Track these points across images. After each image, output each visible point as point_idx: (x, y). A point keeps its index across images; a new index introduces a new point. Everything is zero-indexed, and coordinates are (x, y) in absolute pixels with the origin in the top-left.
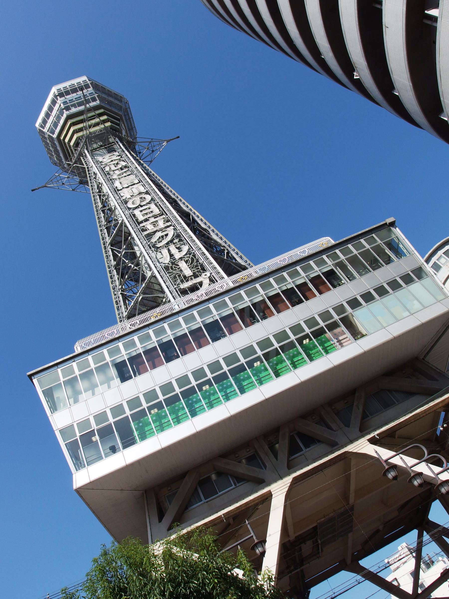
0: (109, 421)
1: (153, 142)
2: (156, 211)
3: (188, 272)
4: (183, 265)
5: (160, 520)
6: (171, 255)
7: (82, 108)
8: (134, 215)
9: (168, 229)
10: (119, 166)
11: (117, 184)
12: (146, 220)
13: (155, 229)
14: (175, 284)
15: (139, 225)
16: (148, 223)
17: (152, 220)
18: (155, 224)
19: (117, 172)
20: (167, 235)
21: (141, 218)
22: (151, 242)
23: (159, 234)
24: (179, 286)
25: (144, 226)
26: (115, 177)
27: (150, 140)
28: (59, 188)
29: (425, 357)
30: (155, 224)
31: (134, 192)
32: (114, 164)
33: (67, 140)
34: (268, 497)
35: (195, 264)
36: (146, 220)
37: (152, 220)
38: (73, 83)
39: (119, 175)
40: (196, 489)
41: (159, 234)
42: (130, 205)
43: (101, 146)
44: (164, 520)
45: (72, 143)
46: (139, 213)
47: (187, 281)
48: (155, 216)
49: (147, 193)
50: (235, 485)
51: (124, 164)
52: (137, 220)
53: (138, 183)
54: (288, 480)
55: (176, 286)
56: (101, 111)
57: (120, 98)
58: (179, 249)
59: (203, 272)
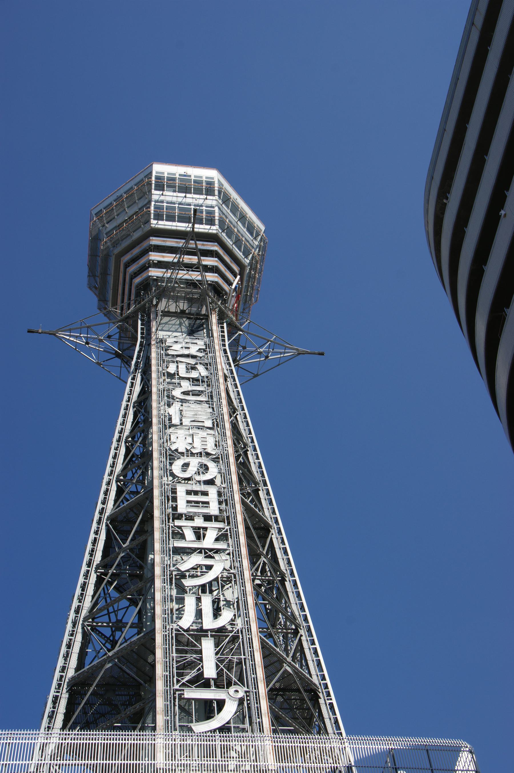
2: (214, 509)
6: (199, 613)
7: (182, 226)
8: (174, 491)
9: (217, 556)
10: (194, 374)
12: (190, 518)
14: (178, 681)
15: (173, 520)
16: (190, 523)
17: (199, 522)
19: (186, 386)
20: (209, 567)
21: (182, 508)
22: (177, 568)
23: (196, 559)
24: (183, 690)
25: (180, 527)
26: (177, 393)
28: (76, 349)
31: (195, 445)
35: (230, 656)
36: (190, 518)
38: (189, 173)
41: (196, 559)
42: (177, 467)
43: (183, 312)
45: (137, 280)
48: (208, 518)
49: (216, 460)
52: (175, 509)
56: (215, 247)
58: (217, 613)
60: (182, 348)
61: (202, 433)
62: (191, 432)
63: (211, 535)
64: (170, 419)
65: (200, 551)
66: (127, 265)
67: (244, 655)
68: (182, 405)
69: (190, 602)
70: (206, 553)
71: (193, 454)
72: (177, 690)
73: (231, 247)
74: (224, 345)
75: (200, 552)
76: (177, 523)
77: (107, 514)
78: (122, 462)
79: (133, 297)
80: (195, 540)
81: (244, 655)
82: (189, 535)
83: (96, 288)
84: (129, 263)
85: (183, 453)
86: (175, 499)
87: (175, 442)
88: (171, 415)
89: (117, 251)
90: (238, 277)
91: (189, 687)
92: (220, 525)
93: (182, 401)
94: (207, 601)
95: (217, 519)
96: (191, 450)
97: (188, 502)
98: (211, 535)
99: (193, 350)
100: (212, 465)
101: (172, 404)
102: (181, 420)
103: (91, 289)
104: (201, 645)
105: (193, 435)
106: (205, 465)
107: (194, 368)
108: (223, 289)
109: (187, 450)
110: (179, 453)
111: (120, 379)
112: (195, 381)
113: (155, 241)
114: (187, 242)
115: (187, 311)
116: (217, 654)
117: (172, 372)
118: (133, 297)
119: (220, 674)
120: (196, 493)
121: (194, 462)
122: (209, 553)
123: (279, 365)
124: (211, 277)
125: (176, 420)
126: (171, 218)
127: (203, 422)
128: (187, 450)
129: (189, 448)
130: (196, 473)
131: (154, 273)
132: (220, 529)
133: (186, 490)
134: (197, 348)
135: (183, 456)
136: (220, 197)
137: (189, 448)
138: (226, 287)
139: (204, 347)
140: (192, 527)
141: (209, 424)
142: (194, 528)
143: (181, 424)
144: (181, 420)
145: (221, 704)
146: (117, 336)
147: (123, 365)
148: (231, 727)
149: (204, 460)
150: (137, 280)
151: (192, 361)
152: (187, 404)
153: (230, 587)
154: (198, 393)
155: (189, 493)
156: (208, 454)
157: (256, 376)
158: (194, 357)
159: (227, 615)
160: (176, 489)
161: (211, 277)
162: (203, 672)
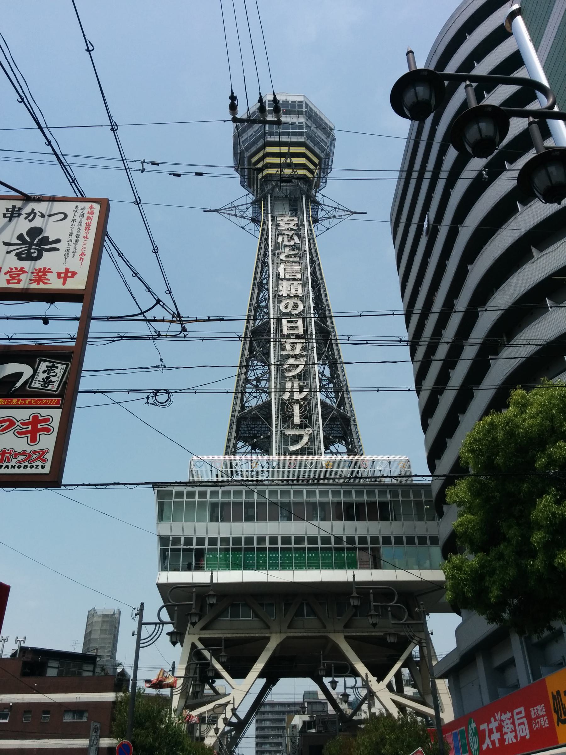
1: (338, 209)
2: (300, 331)
3: (297, 420)
4: (296, 409)
9: (302, 359)
10: (292, 243)
13: (291, 353)
14: (283, 426)
18: (293, 344)
19: (287, 250)
20: (298, 365)
21: (285, 331)
23: (292, 361)
27: (335, 205)
30: (293, 344)
31: (292, 291)
32: (288, 235)
34: (268, 639)
39: (287, 256)
40: (227, 609)
41: (292, 361)
46: (286, 322)
47: (293, 428)
48: (298, 336)
49: (302, 299)
50: (253, 618)
53: (300, 280)
54: (284, 636)
57: (327, 130)
58: (301, 391)
61: (296, 283)
62: (290, 283)
63: (298, 347)
65: (292, 356)
72: (283, 430)
73: (313, 148)
75: (293, 357)
77: (250, 329)
79: (259, 187)
82: (288, 346)
94: (296, 384)
98: (298, 347)
99: (291, 226)
100: (300, 303)
108: (309, 178)
109: (288, 295)
110: (284, 297)
112: (293, 248)
113: (269, 149)
114: (286, 160)
118: (259, 187)
121: (291, 302)
122: (297, 357)
125: (282, 276)
128: (288, 295)
132: (303, 343)
134: (294, 223)
136: (306, 116)
137: (289, 293)
138: (310, 175)
141: (299, 276)
145: (301, 437)
147: (256, 229)
149: (296, 300)
157: (328, 229)
161: (301, 172)
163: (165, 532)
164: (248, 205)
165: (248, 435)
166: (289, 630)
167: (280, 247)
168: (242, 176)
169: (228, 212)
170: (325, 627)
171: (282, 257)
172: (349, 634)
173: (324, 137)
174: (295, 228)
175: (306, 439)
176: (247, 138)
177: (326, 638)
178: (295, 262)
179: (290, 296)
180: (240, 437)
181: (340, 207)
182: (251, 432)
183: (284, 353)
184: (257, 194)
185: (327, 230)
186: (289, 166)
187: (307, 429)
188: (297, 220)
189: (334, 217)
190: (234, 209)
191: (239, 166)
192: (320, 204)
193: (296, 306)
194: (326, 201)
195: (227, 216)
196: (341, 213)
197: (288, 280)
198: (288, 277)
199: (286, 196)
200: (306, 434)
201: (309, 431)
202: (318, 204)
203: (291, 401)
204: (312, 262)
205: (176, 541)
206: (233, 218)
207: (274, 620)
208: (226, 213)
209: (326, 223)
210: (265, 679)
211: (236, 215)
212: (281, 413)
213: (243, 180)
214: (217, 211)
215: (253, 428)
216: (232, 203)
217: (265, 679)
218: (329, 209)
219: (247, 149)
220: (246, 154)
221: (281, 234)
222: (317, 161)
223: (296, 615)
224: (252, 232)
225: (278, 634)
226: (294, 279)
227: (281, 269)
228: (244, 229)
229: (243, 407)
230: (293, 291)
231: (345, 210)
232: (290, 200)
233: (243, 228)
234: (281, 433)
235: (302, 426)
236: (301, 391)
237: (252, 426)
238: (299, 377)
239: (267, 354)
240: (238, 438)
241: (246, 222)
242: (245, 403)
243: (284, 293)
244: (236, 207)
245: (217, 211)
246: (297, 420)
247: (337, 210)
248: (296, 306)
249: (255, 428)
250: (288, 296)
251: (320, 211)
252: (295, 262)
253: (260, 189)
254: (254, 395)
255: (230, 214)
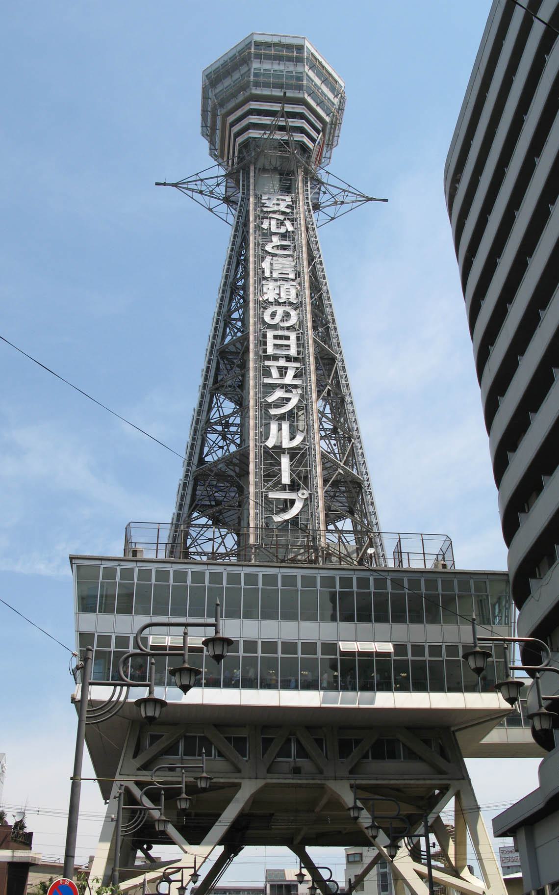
0: (129, 649)
2: (293, 352)
3: (286, 479)
4: (285, 461)
5: (135, 756)
6: (280, 437)
7: (278, 93)
8: (265, 336)
9: (294, 391)
10: (282, 230)
11: (266, 265)
14: (265, 486)
18: (282, 371)
19: (276, 240)
20: (289, 399)
21: (270, 350)
22: (265, 400)
23: (279, 394)
25: (268, 367)
27: (345, 187)
29: (457, 730)
30: (282, 371)
33: (236, 129)
34: (237, 787)
37: (282, 363)
41: (279, 394)
44: (139, 757)
45: (240, 140)
48: (289, 359)
49: (297, 306)
50: (215, 757)
51: (290, 228)
52: (265, 351)
53: (293, 280)
54: (260, 783)
55: (263, 490)
58: (292, 438)
59: (303, 488)
60: (274, 204)
61: (287, 285)
62: (278, 283)
63: (291, 373)
64: (263, 272)
65: (282, 386)
66: (232, 125)
67: (310, 467)
68: (272, 259)
69: (274, 427)
70: (286, 388)
71: (279, 304)
74: (307, 199)
75: (282, 388)
76: (267, 363)
77: (217, 348)
78: (227, 303)
79: (236, 154)
80: (279, 377)
81: (310, 467)
82: (275, 373)
83: (207, 135)
84: (233, 123)
85: (272, 302)
86: (265, 343)
87: (266, 293)
88: (264, 269)
89: (224, 111)
90: (321, 133)
91: (271, 490)
92: (297, 365)
93: (274, 255)
94: (285, 426)
95: (296, 360)
96: (279, 300)
97: (275, 345)
98: (291, 373)
99: (282, 208)
100: (293, 313)
101: (265, 257)
102: (271, 273)
103: (204, 137)
104: (280, 459)
105: (280, 287)
106: (289, 313)
107: (282, 224)
108: (308, 147)
111: (226, 222)
112: (284, 236)
113: (254, 105)
115: (279, 168)
116: (291, 466)
117: (266, 228)
118: (236, 154)
119: (293, 481)
120: (281, 337)
121: (280, 310)
122: (287, 388)
123: (352, 209)
124: (298, 137)
125: (267, 274)
126: (267, 85)
127: (288, 274)
129: (276, 299)
130: (281, 320)
131: (254, 134)
132: (297, 368)
133: (274, 335)
135: (272, 305)
138: (310, 145)
139: (291, 203)
140: (277, 366)
141: (292, 276)
142: (278, 367)
143: (271, 276)
144: (271, 273)
145: (293, 502)
146: (224, 184)
147: (229, 212)
148: (257, 657)
149: (288, 309)
150: (240, 140)
151: (281, 217)
152: (277, 258)
153: (303, 414)
154: (284, 248)
155: (275, 337)
156: (291, 304)
157: (333, 219)
158: (283, 213)
159: (299, 438)
160: (266, 334)
161: (298, 137)
162: (281, 479)
163: (87, 628)
164: (219, 178)
165: (208, 503)
166: (269, 775)
167: (267, 235)
168: (212, 142)
169: (190, 187)
170: (321, 772)
171: (268, 248)
172: (358, 782)
173: (331, 96)
174: (288, 211)
175: (298, 506)
176: (223, 89)
177: (322, 787)
178: (289, 256)
179: (279, 302)
180: (197, 505)
181: (351, 190)
182: (212, 498)
183: (267, 381)
184: (233, 165)
185: (331, 220)
186: (282, 128)
187: (301, 491)
188: (290, 200)
189: (342, 203)
190: (199, 183)
191: (210, 130)
192: (323, 183)
193: (287, 315)
194: (332, 180)
195: (189, 193)
196: (352, 198)
197: (276, 280)
198: (275, 275)
199: (275, 169)
200: (299, 498)
201: (304, 494)
202: (321, 183)
203: (279, 449)
204: (311, 258)
205: (105, 640)
206: (197, 196)
207: (247, 761)
208: (188, 189)
209: (330, 211)
210: (223, 846)
211: (201, 192)
212: (263, 467)
213: (212, 147)
214: (175, 185)
215: (216, 492)
216: (197, 174)
217: (223, 846)
218: (335, 191)
219: (221, 105)
220: (220, 111)
221: (267, 218)
222: (319, 126)
223: (279, 755)
224: (224, 216)
225: (254, 781)
226: (286, 280)
227: (266, 265)
228: (212, 211)
229: (201, 461)
230: (282, 295)
231: (357, 194)
232: (281, 174)
233: (210, 210)
234: (262, 497)
235: (293, 487)
236: (292, 438)
237: (216, 489)
238: (290, 416)
239: (243, 385)
240: (193, 507)
241: (214, 202)
242: (206, 456)
243: (271, 296)
244: (202, 180)
245: (175, 185)
246: (286, 479)
247: (346, 193)
248: (287, 315)
249: (220, 493)
250: (277, 303)
251: (321, 195)
252: (289, 256)
253: (239, 157)
254: (220, 444)
255: (193, 190)
